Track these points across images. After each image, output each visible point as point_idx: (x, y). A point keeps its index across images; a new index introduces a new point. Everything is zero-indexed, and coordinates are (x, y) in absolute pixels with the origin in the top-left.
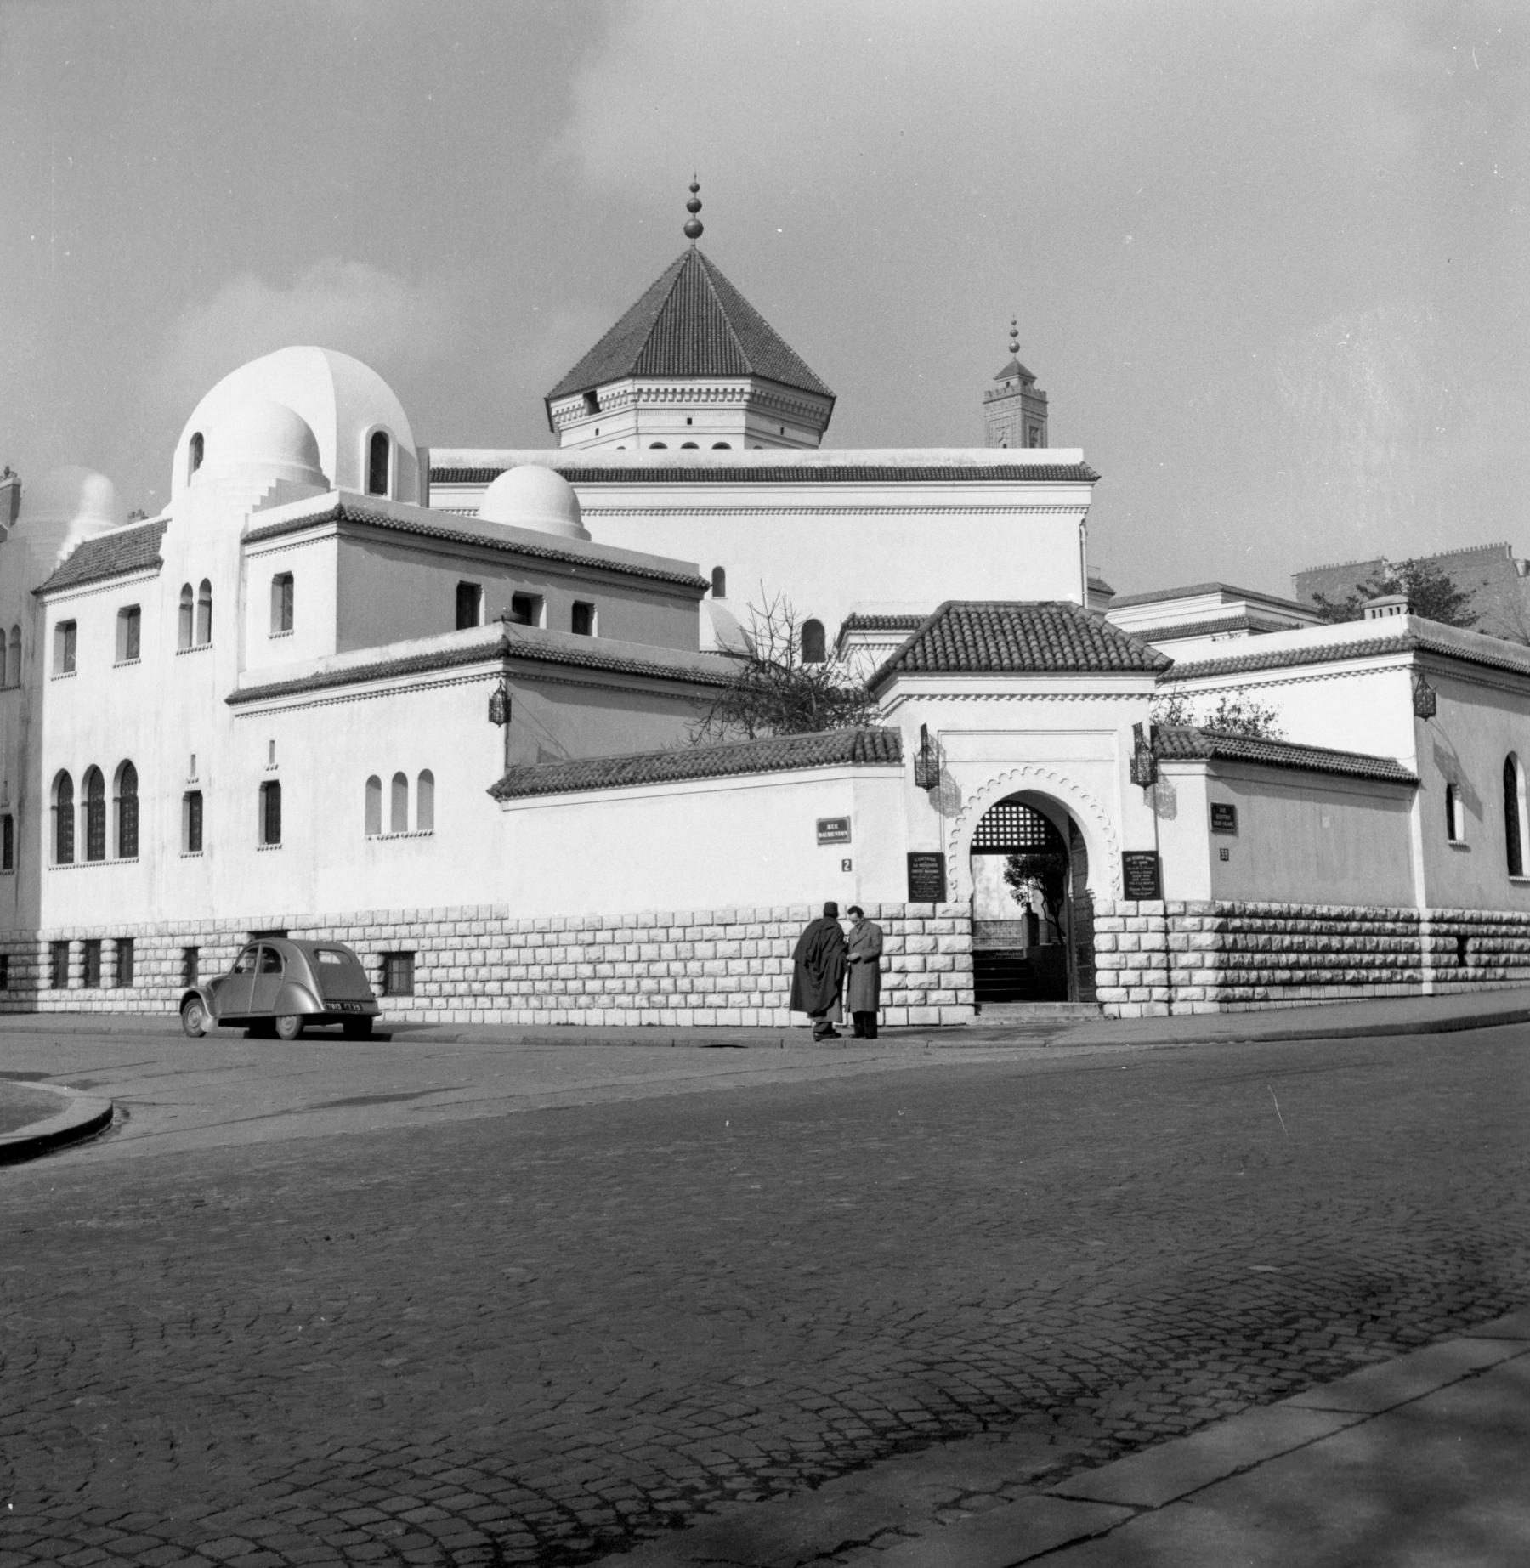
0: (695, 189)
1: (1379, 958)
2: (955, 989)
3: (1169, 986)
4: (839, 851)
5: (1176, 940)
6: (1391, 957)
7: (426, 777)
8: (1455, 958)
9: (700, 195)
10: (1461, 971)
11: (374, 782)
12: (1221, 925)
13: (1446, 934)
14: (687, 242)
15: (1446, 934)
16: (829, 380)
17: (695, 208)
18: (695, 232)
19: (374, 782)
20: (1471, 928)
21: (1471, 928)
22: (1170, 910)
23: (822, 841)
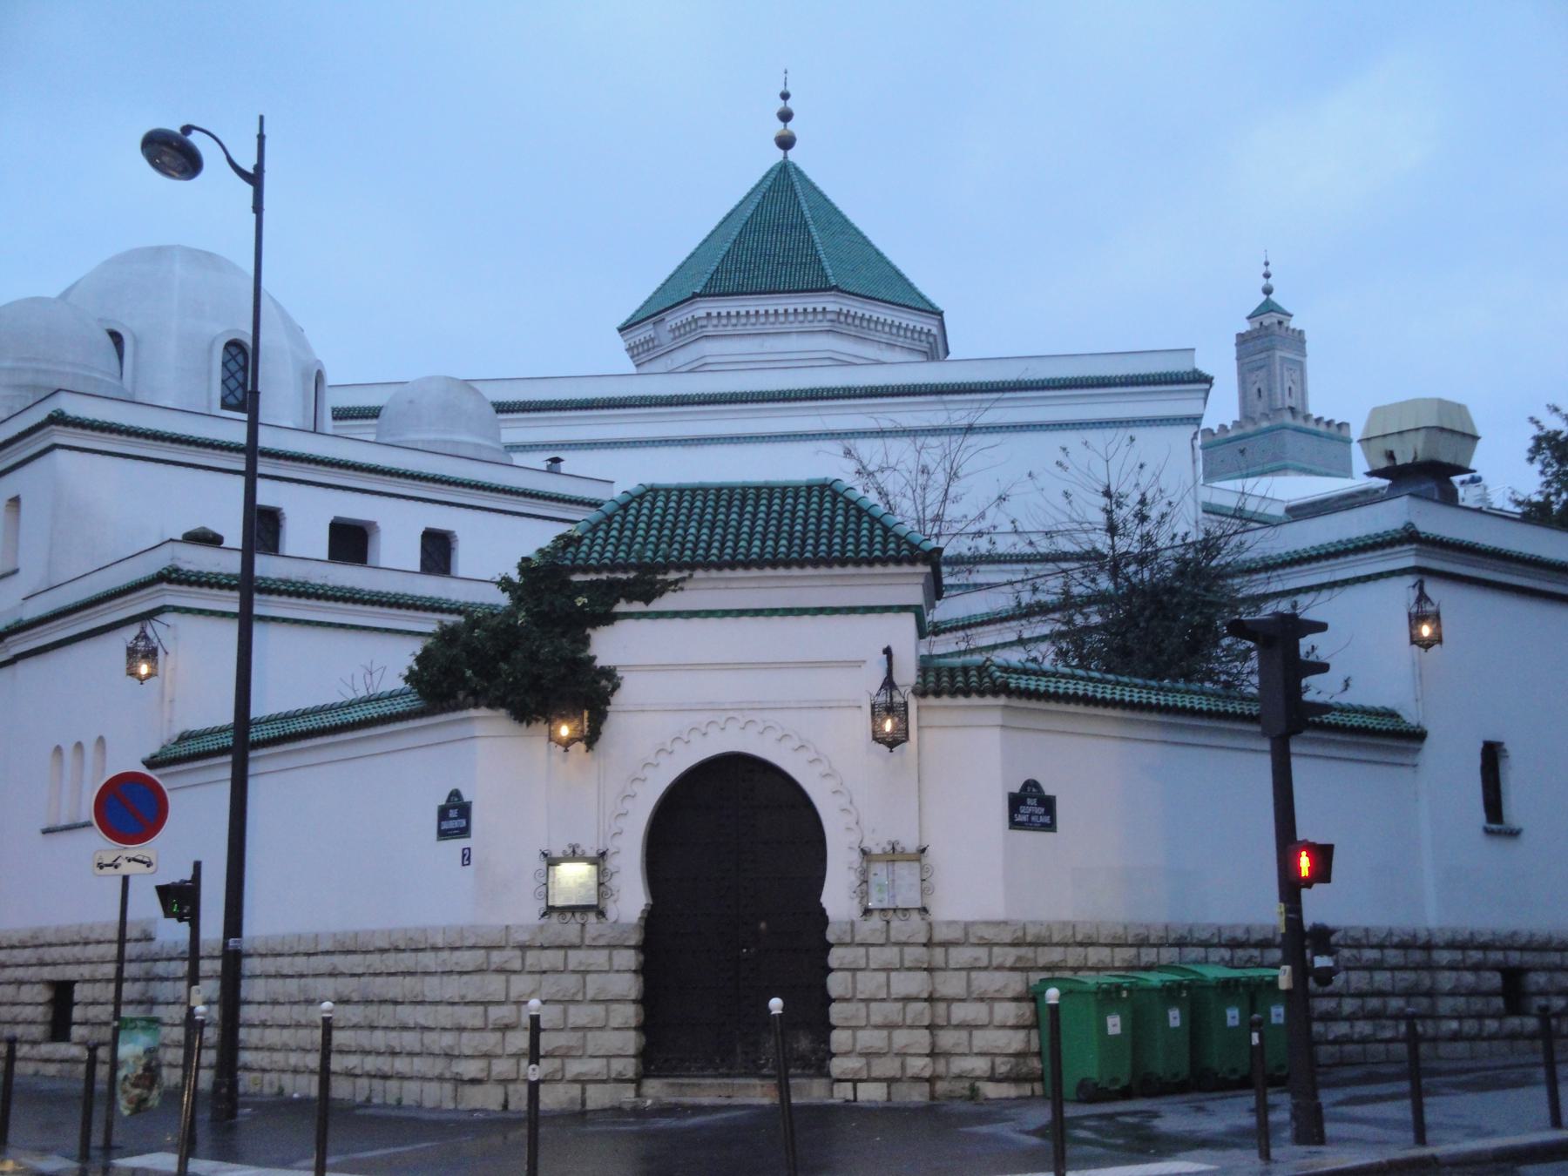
0: (785, 96)
1: (1349, 1005)
2: (608, 1057)
3: (933, 1054)
4: (457, 845)
5: (951, 985)
6: (1374, 1003)
7: (101, 740)
8: (1499, 1002)
9: (790, 103)
10: (1514, 1022)
11: (58, 749)
12: (1019, 958)
13: (1476, 968)
14: (777, 155)
15: (1476, 968)
16: (939, 303)
17: (785, 116)
18: (786, 142)
19: (58, 749)
20: (1529, 957)
21: (1529, 957)
22: (941, 934)
23: (443, 834)
